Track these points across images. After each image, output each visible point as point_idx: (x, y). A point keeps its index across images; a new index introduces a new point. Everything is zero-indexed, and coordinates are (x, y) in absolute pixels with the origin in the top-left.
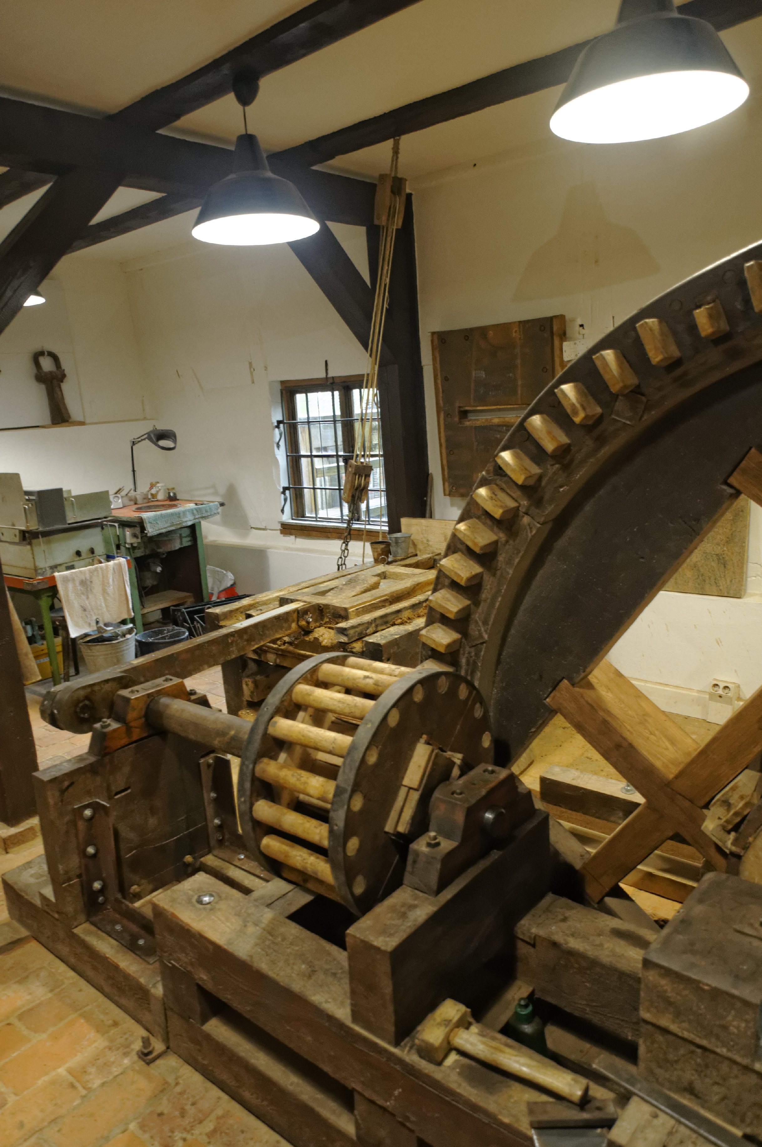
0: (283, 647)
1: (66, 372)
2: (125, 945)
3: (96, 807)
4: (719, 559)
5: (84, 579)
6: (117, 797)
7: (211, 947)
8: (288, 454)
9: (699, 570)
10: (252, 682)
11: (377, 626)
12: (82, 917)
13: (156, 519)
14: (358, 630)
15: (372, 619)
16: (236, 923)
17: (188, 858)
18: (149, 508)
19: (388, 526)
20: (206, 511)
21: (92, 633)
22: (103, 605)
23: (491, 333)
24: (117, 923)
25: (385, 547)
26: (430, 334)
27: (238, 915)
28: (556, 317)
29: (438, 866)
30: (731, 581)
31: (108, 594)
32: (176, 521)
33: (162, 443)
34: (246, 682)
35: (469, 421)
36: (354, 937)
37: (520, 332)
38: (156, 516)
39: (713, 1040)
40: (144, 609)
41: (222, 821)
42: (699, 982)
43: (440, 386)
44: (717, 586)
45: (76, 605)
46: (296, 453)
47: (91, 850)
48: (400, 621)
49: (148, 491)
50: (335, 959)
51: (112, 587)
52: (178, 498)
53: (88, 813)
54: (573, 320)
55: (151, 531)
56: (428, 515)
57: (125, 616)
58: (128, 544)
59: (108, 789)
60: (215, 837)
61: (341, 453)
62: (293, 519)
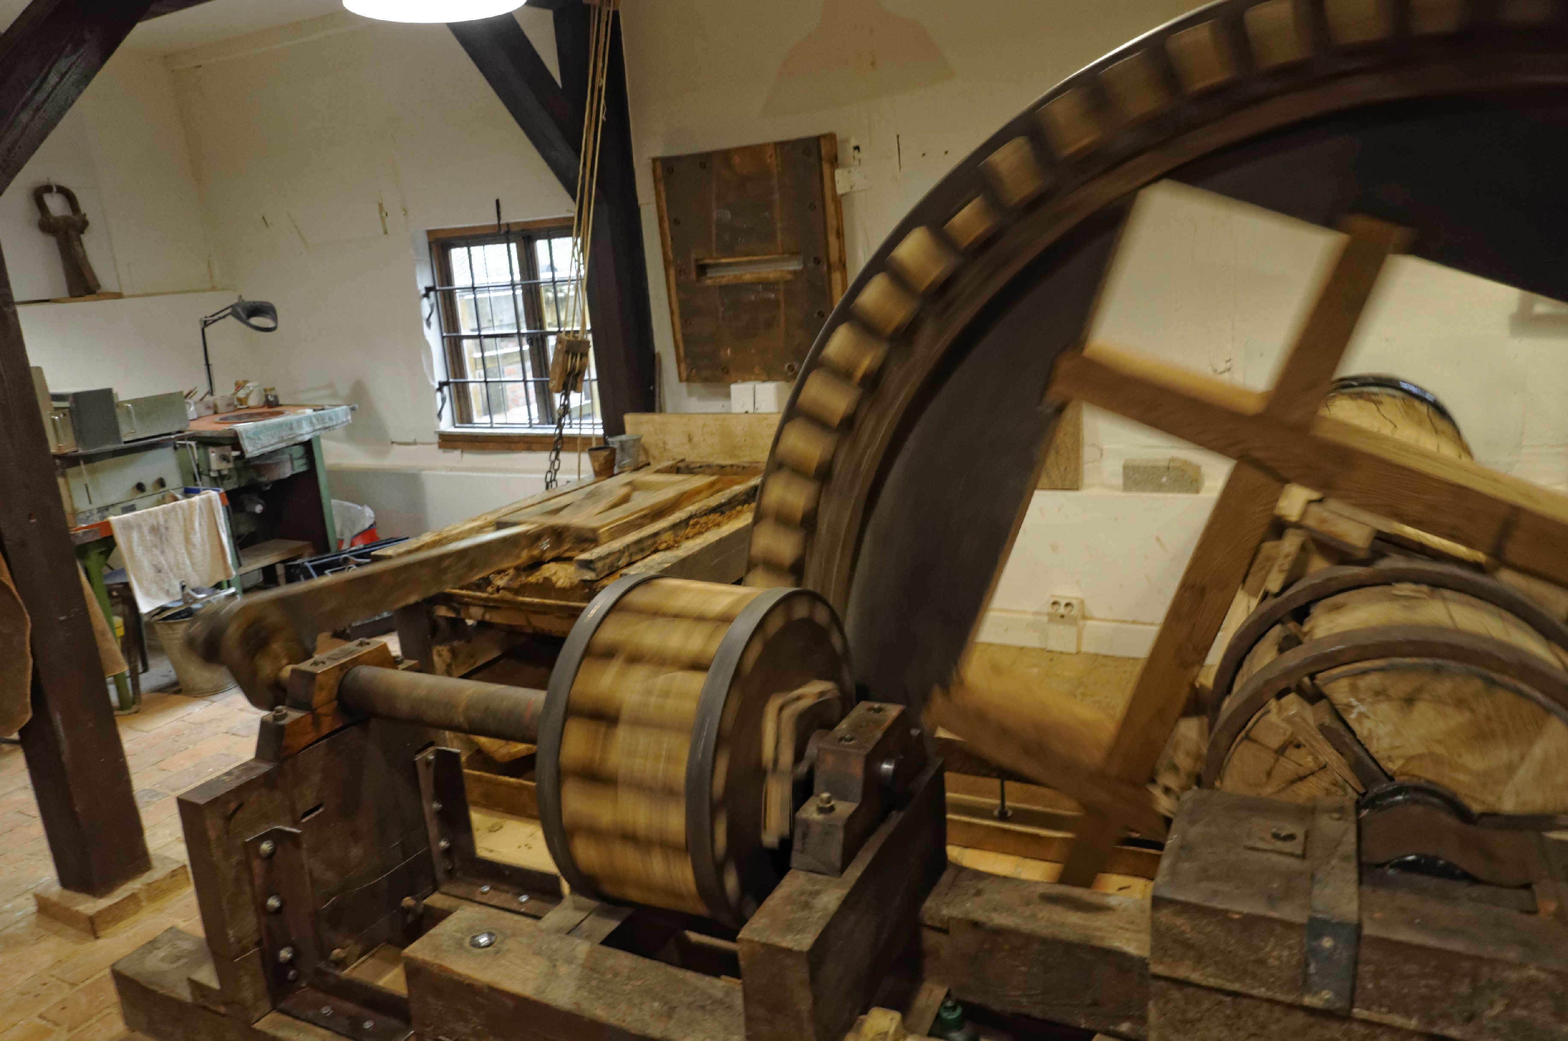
0: (496, 596)
1: (89, 217)
2: (344, 1032)
3: (277, 837)
5: (155, 524)
6: (304, 820)
7: (510, 1003)
8: (445, 334)
10: (449, 651)
11: (631, 555)
12: (265, 1005)
13: (257, 432)
14: (608, 561)
15: (625, 545)
16: (540, 965)
17: (408, 901)
18: (240, 419)
19: (603, 428)
20: (331, 419)
21: (170, 605)
22: (187, 562)
23: (737, 159)
24: (324, 1004)
25: (609, 455)
26: (650, 161)
27: (538, 953)
28: (824, 136)
29: (841, 835)
31: (194, 545)
32: (286, 434)
33: (255, 321)
34: (438, 652)
35: (711, 278)
36: (751, 941)
38: (257, 427)
39: (1248, 981)
40: (241, 568)
41: (450, 841)
42: (1228, 911)
43: (668, 232)
45: (146, 564)
46: (454, 332)
47: (273, 902)
48: (664, 546)
49: (234, 394)
50: (696, 989)
51: (198, 535)
52: (281, 402)
53: (266, 847)
54: (846, 141)
55: (251, 450)
56: (657, 410)
57: (221, 577)
58: (214, 471)
59: (293, 810)
60: (441, 866)
61: (524, 330)
62: (456, 427)
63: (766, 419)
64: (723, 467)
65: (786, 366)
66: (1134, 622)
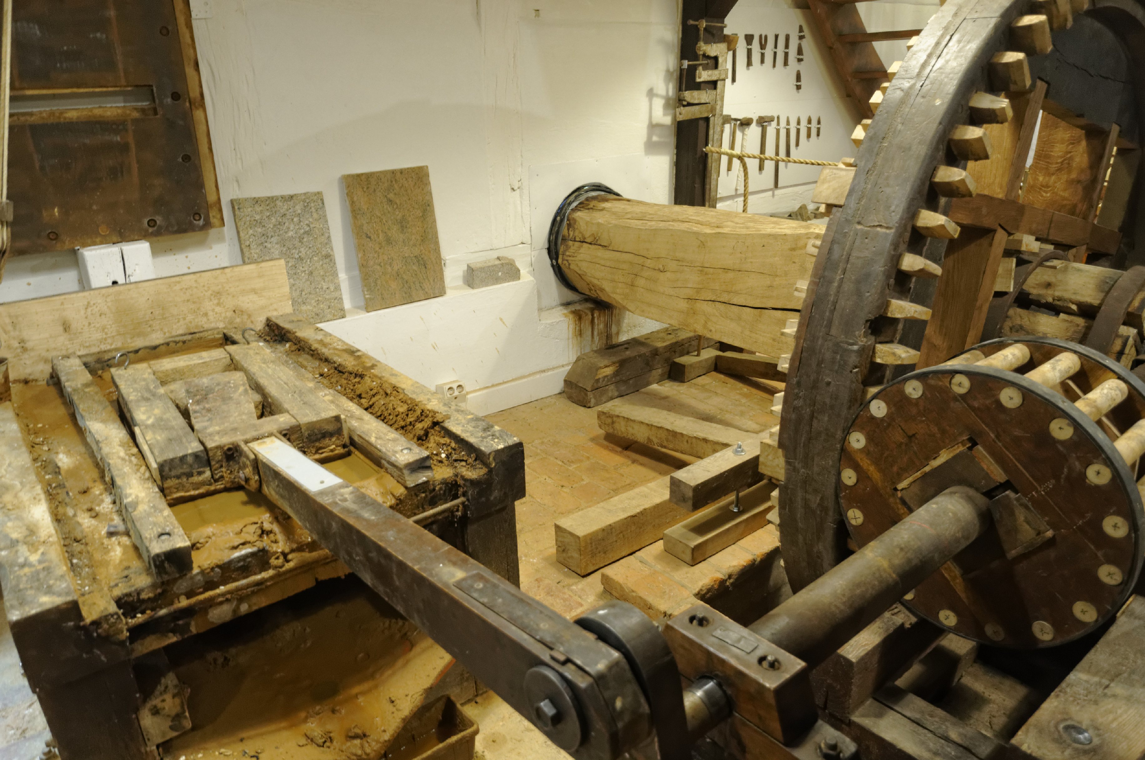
4: (418, 261)
9: (402, 278)
44: (423, 290)
63: (179, 282)
64: (155, 348)
65: (146, 221)
66: (493, 386)
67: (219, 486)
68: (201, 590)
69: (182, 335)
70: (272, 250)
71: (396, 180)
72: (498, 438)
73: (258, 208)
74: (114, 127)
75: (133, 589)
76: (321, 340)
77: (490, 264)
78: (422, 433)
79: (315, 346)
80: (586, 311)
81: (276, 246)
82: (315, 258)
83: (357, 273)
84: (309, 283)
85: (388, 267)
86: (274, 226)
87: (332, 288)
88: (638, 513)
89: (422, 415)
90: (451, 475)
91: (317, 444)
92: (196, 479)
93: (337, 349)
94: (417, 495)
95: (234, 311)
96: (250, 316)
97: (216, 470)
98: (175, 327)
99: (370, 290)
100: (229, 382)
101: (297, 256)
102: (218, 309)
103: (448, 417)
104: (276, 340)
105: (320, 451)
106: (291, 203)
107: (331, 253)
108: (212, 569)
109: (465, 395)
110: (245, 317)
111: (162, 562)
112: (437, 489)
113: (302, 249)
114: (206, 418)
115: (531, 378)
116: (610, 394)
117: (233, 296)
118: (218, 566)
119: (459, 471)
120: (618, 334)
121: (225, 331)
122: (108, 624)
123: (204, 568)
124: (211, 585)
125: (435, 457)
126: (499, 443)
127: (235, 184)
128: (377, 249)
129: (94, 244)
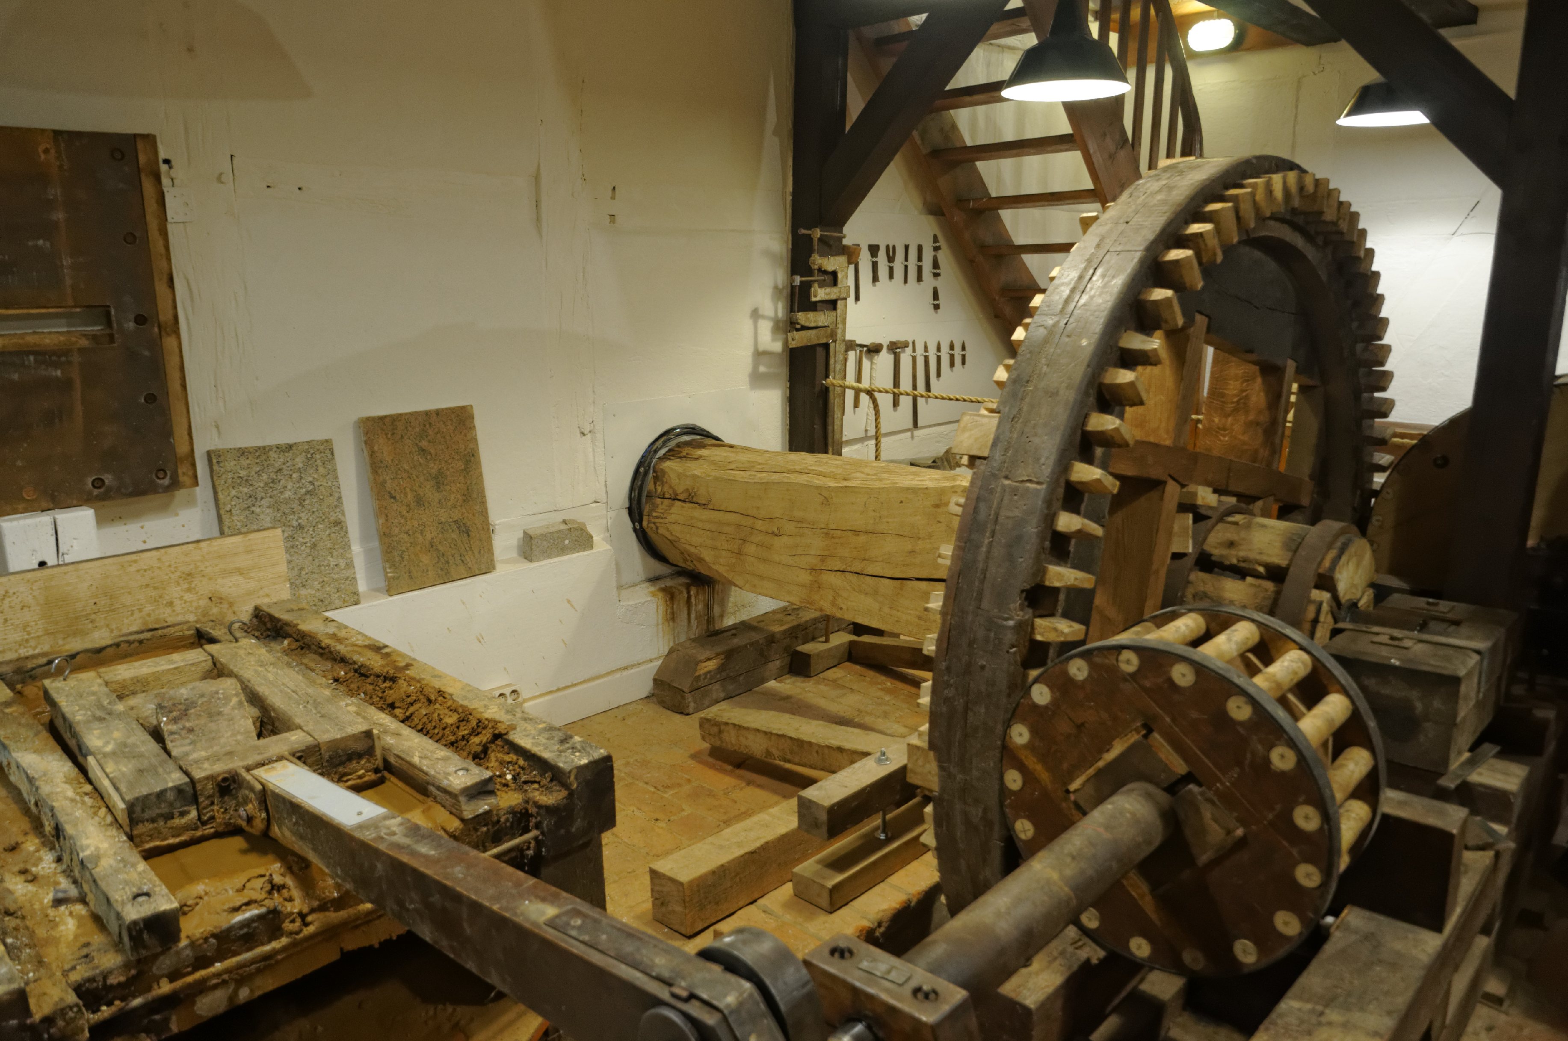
30: (480, 552)
37: (58, 152)
63: (135, 561)
64: (99, 650)
65: (89, 481)
66: (559, 690)
67: (208, 830)
68: (189, 969)
69: (137, 633)
70: (262, 516)
71: (430, 424)
72: (579, 751)
73: (244, 462)
74: (54, 358)
75: (98, 971)
76: (334, 635)
77: (554, 530)
78: (479, 749)
79: (326, 641)
80: (680, 588)
81: (268, 511)
82: (320, 526)
83: (376, 544)
84: (310, 558)
85: (419, 536)
86: (266, 484)
87: (342, 564)
88: (759, 848)
89: (478, 726)
90: (520, 801)
91: (341, 769)
92: (178, 822)
93: (356, 645)
94: (476, 830)
95: (210, 598)
96: (231, 605)
97: (205, 808)
98: (126, 621)
99: (393, 566)
100: (217, 693)
101: (295, 523)
102: (188, 596)
103: (513, 727)
104: (268, 636)
105: (345, 779)
106: (289, 455)
107: (342, 518)
108: (206, 939)
109: (521, 704)
110: (225, 606)
111: (140, 932)
112: (503, 820)
113: (302, 515)
114: (188, 741)
115: (610, 678)
116: (715, 696)
117: (210, 579)
118: (214, 935)
119: (531, 795)
120: (722, 616)
121: (198, 626)
122: (65, 1020)
123: (194, 939)
124: (202, 962)
125: (499, 780)
126: (580, 758)
127: (214, 430)
128: (404, 512)
129: (15, 512)
